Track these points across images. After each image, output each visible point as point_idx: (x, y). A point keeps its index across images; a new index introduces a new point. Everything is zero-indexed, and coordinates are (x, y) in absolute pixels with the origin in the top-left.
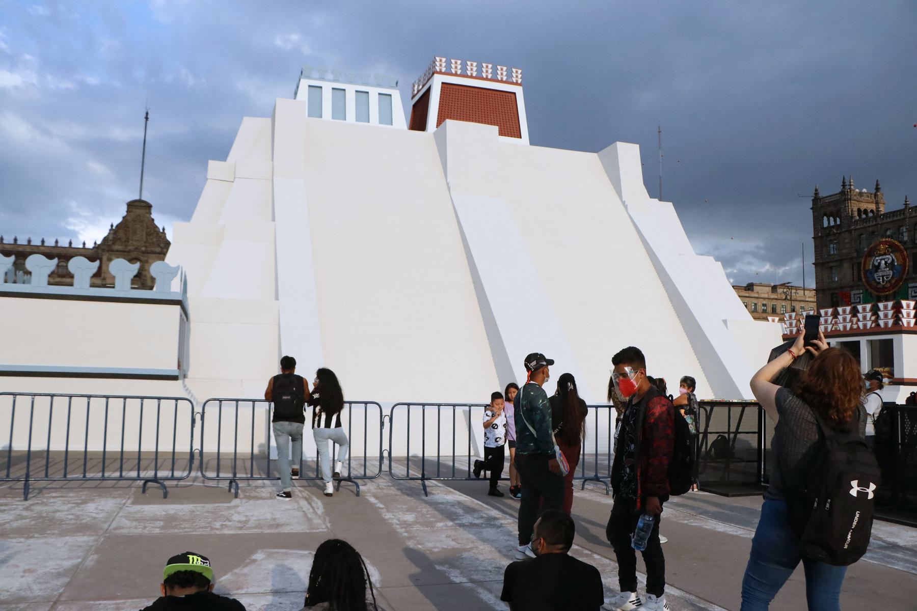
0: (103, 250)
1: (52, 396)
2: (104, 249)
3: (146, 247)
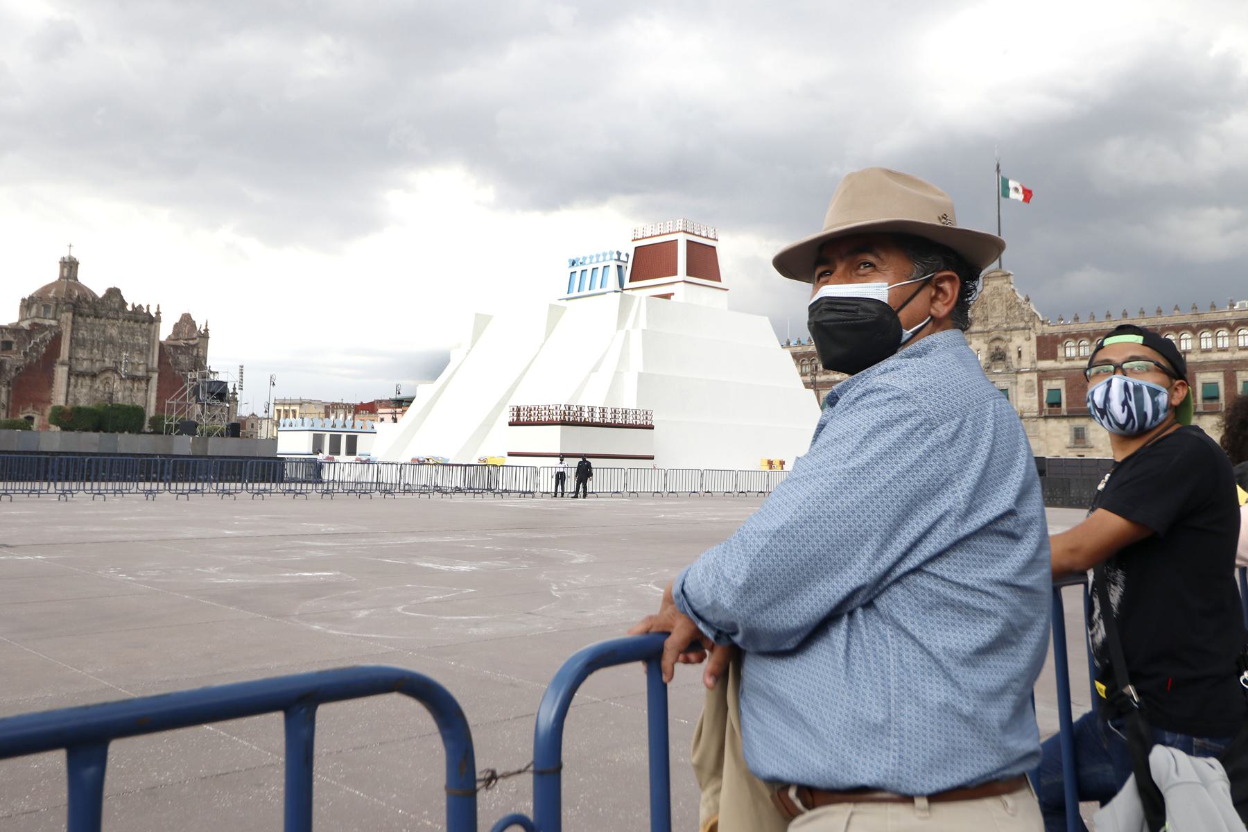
3: (1008, 323)
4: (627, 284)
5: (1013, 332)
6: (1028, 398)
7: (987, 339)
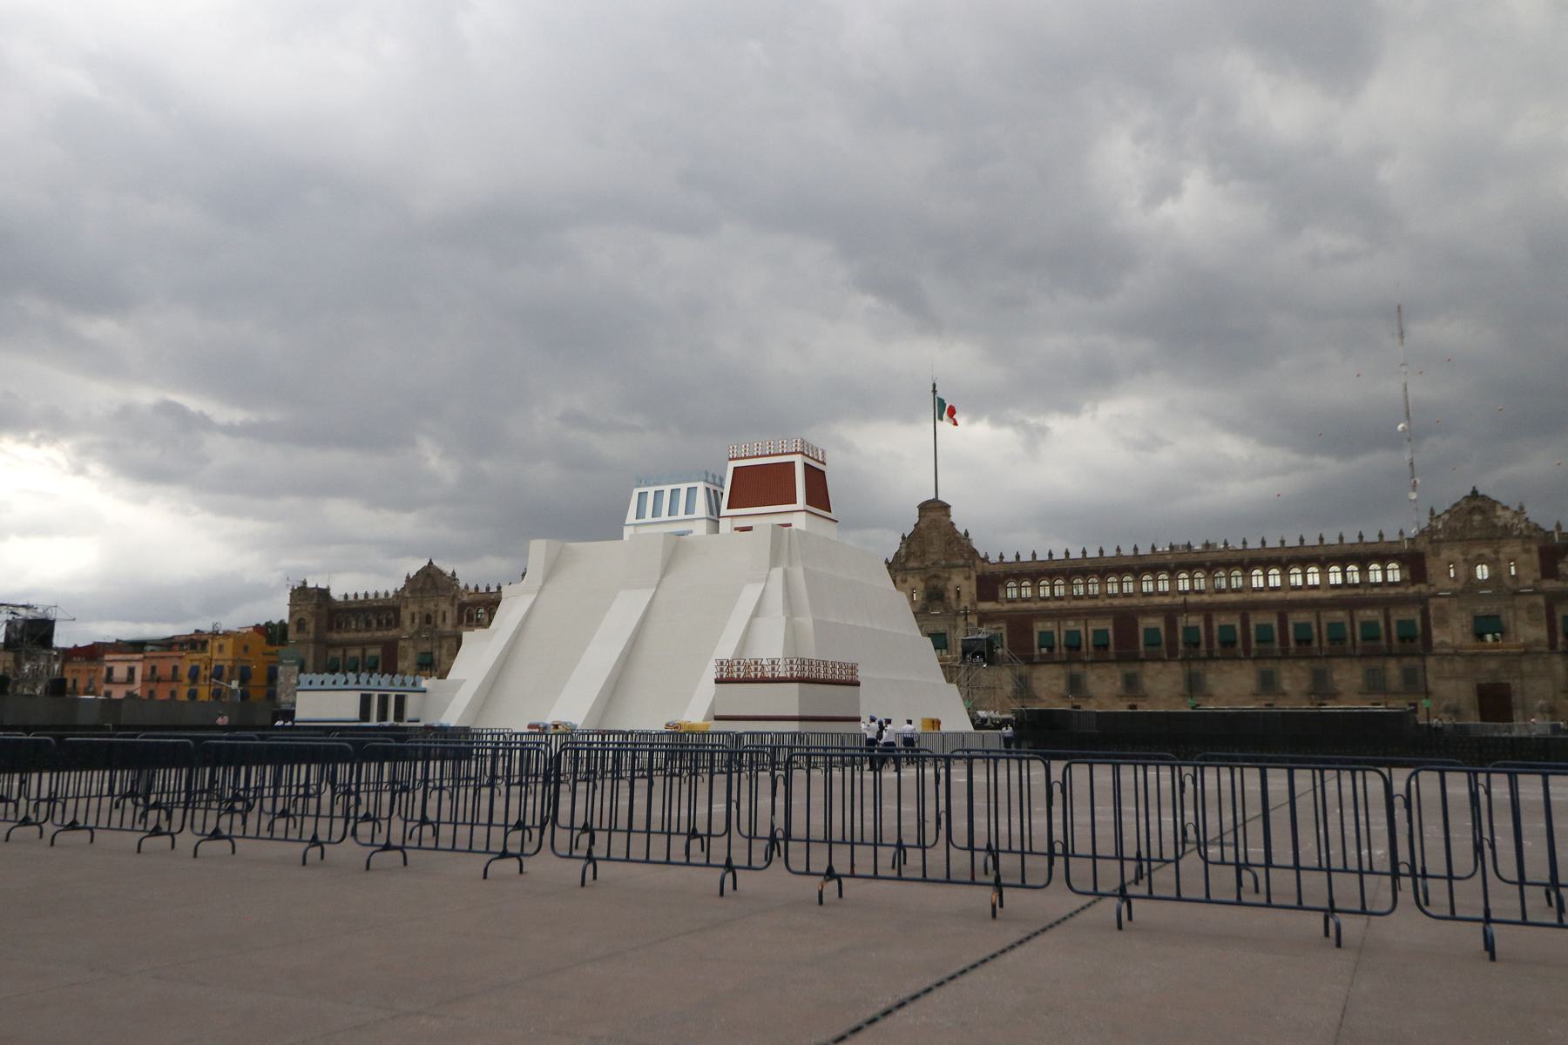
3: (946, 560)
4: (724, 511)
5: (953, 570)
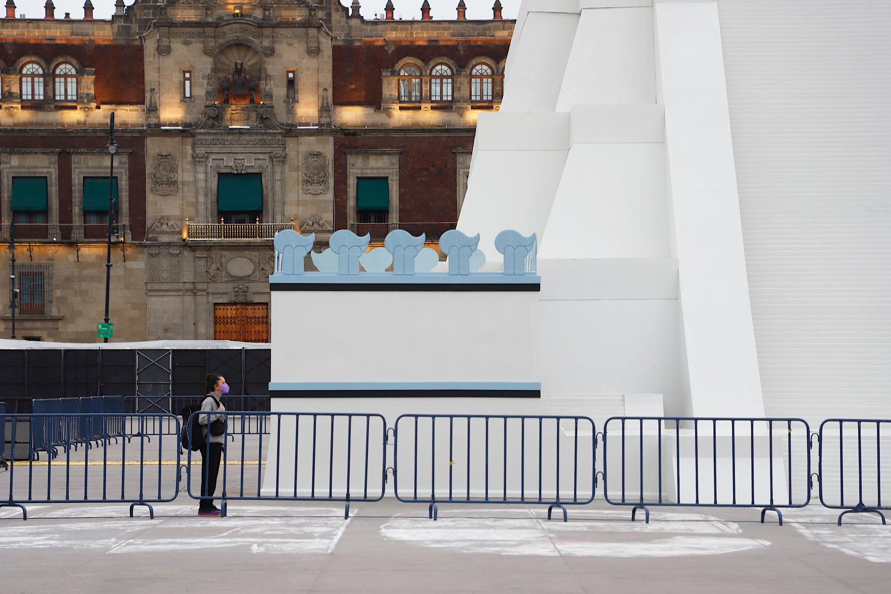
0: (144, 25)
1: (451, 417)
2: (147, 21)
6: (309, 197)
7: (211, 43)
